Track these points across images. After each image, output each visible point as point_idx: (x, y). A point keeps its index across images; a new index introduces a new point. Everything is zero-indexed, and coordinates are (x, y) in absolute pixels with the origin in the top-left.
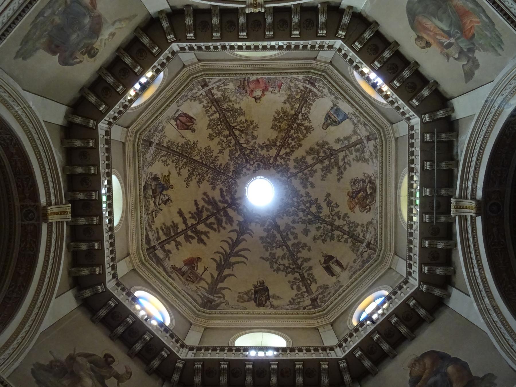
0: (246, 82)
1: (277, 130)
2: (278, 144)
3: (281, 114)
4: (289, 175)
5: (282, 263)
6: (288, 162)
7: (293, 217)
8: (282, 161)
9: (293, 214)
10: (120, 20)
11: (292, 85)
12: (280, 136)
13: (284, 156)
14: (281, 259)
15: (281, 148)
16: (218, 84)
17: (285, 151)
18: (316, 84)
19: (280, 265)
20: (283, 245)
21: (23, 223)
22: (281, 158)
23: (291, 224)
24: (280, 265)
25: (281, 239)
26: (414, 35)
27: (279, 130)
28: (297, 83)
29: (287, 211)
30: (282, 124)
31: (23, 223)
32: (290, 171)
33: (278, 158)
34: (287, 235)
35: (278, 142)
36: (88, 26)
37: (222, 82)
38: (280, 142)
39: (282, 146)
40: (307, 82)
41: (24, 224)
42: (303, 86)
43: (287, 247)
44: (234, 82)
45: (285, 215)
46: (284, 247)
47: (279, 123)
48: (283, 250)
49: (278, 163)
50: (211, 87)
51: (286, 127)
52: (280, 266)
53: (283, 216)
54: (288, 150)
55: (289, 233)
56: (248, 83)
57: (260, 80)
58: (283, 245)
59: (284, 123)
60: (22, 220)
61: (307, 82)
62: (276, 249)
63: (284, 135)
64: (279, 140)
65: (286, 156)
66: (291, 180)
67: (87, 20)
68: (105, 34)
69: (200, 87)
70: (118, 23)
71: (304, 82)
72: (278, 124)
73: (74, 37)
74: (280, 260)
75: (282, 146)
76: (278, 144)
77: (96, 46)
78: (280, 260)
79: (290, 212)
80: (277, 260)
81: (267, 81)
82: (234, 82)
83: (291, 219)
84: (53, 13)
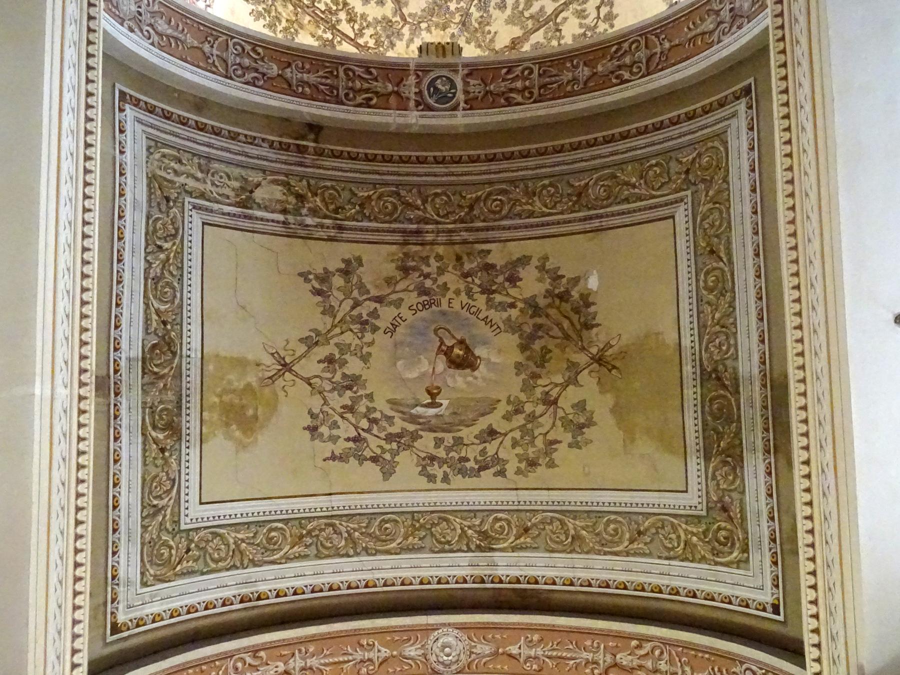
1: (296, 31)
2: (330, 37)
3: (260, 9)
4: (398, 19)
5: (594, 14)
6: (370, 19)
7: (491, 9)
8: (368, 32)
9: (485, 11)
12: (312, 28)
13: (356, 27)
14: (585, 18)
15: (339, 31)
17: (344, 22)
19: (598, 17)
20: (556, 24)
21: (462, 105)
22: (360, 34)
23: (508, 12)
24: (598, 17)
25: (542, 31)
27: (295, 25)
29: (480, 23)
30: (284, 14)
31: (462, 105)
32: (390, 15)
33: (361, 41)
34: (532, 17)
35: (325, 36)
38: (324, 32)
39: (333, 28)
41: (466, 102)
43: (557, 13)
45: (487, 28)
46: (558, 20)
47: (280, 22)
48: (565, 19)
49: (371, 43)
51: (291, 7)
52: (602, 16)
53: (489, 32)
54: (342, 15)
55: (527, 14)
58: (556, 24)
59: (280, 9)
60: (455, 108)
62: (563, 37)
63: (308, 18)
64: (320, 32)
65: (355, 21)
66: (410, 15)
72: (284, 24)
74: (587, 21)
75: (333, 28)
76: (330, 37)
78: (587, 21)
79: (482, 17)
80: (589, 28)
83: (495, 13)
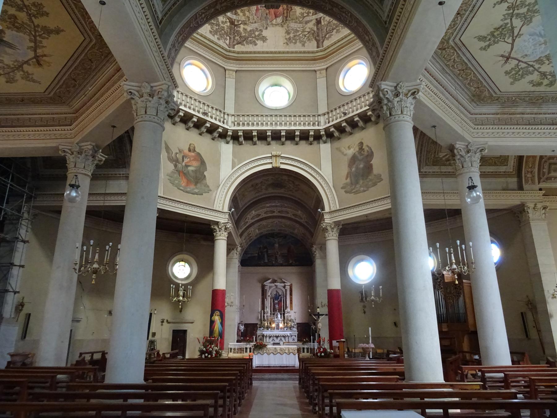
0: (285, 15)
10: (343, 153)
11: (247, 13)
16: (308, 19)
18: (229, 24)
26: (197, 150)
28: (243, 18)
36: (355, 166)
37: (304, 20)
40: (236, 23)
42: (239, 15)
44: (295, 17)
50: (314, 16)
56: (284, 13)
57: (274, 16)
61: (236, 23)
67: (353, 169)
68: (350, 152)
69: (323, 23)
70: (345, 153)
71: (238, 21)
73: (362, 166)
77: (357, 149)
81: (268, 16)
82: (295, 17)
84: (361, 187)
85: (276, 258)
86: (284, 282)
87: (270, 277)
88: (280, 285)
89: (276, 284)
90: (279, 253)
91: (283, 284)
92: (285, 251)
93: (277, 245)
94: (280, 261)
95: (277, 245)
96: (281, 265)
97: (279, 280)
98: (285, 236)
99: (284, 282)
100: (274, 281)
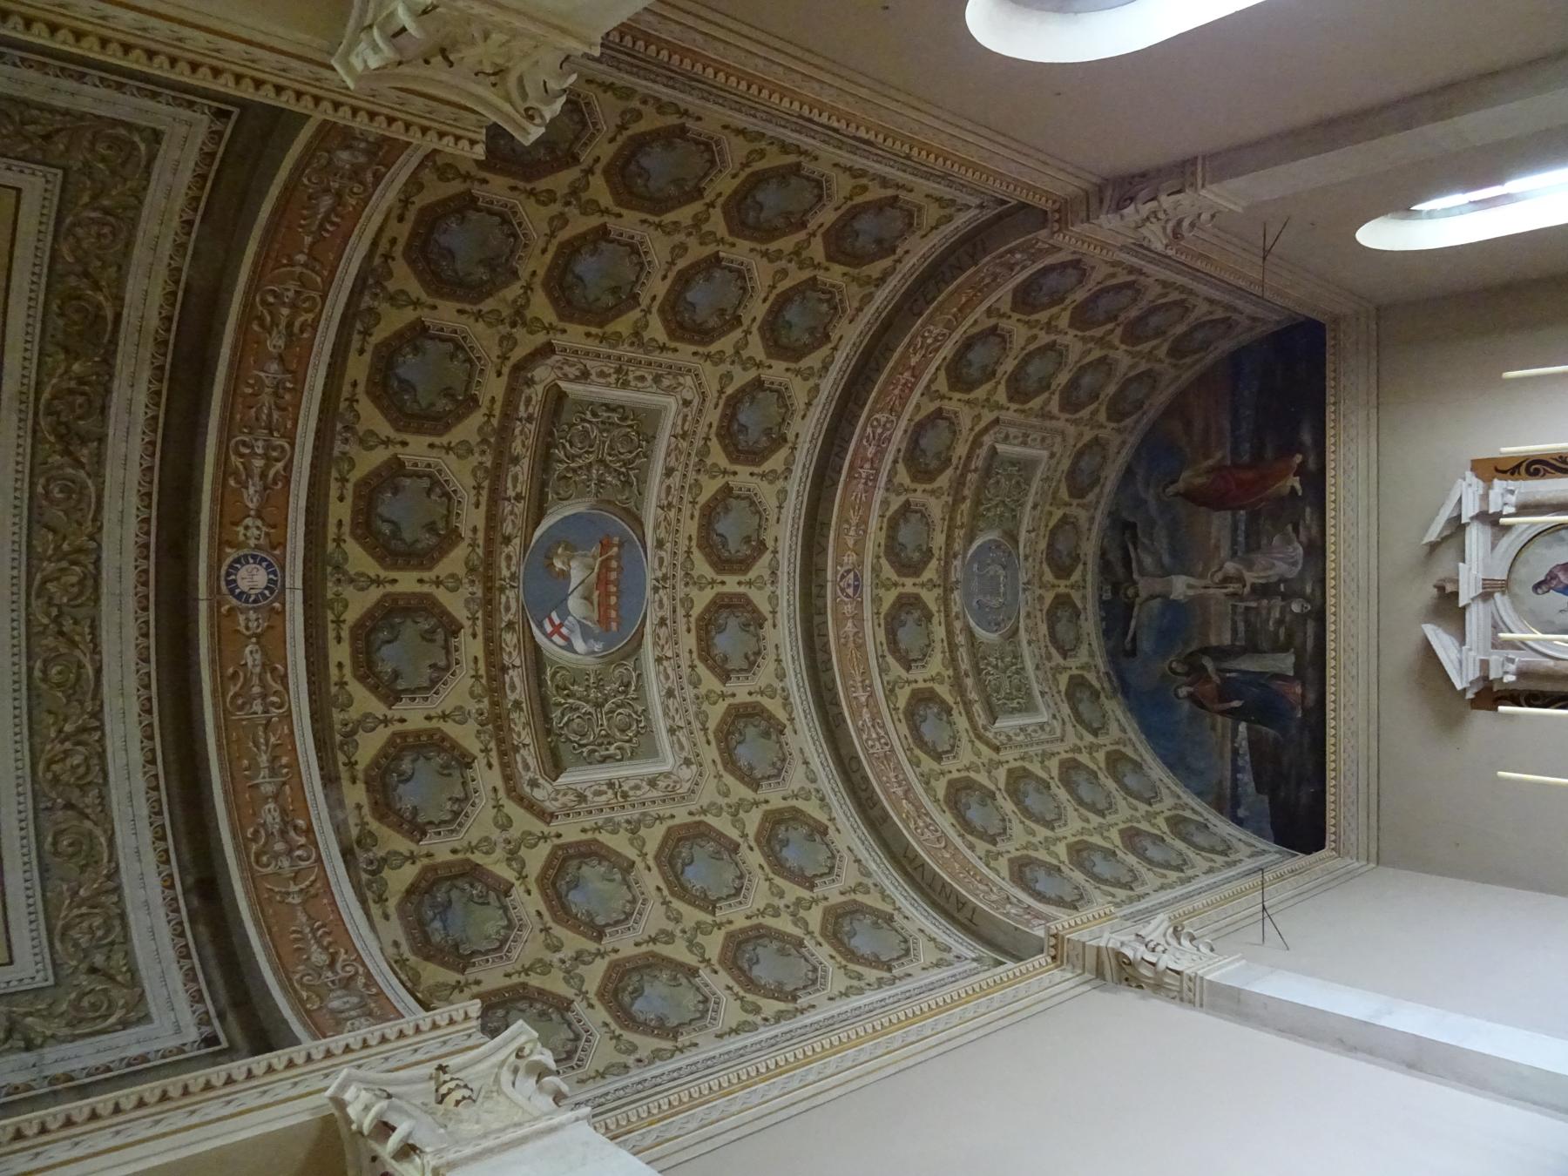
85: (1263, 591)
86: (1457, 527)
87: (1402, 653)
88: (1478, 561)
89: (1467, 592)
90: (1230, 567)
91: (1476, 537)
92: (1219, 525)
93: (1180, 587)
94: (1281, 560)
95: (1180, 587)
96: (1316, 551)
97: (1440, 571)
98: (1124, 530)
99: (1457, 527)
100: (1448, 608)
